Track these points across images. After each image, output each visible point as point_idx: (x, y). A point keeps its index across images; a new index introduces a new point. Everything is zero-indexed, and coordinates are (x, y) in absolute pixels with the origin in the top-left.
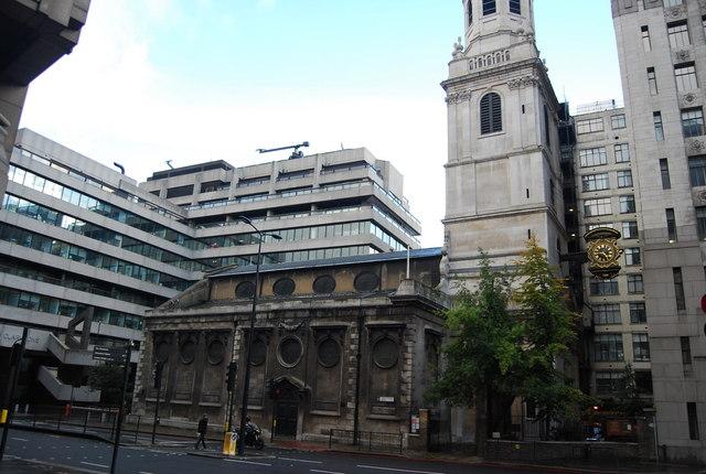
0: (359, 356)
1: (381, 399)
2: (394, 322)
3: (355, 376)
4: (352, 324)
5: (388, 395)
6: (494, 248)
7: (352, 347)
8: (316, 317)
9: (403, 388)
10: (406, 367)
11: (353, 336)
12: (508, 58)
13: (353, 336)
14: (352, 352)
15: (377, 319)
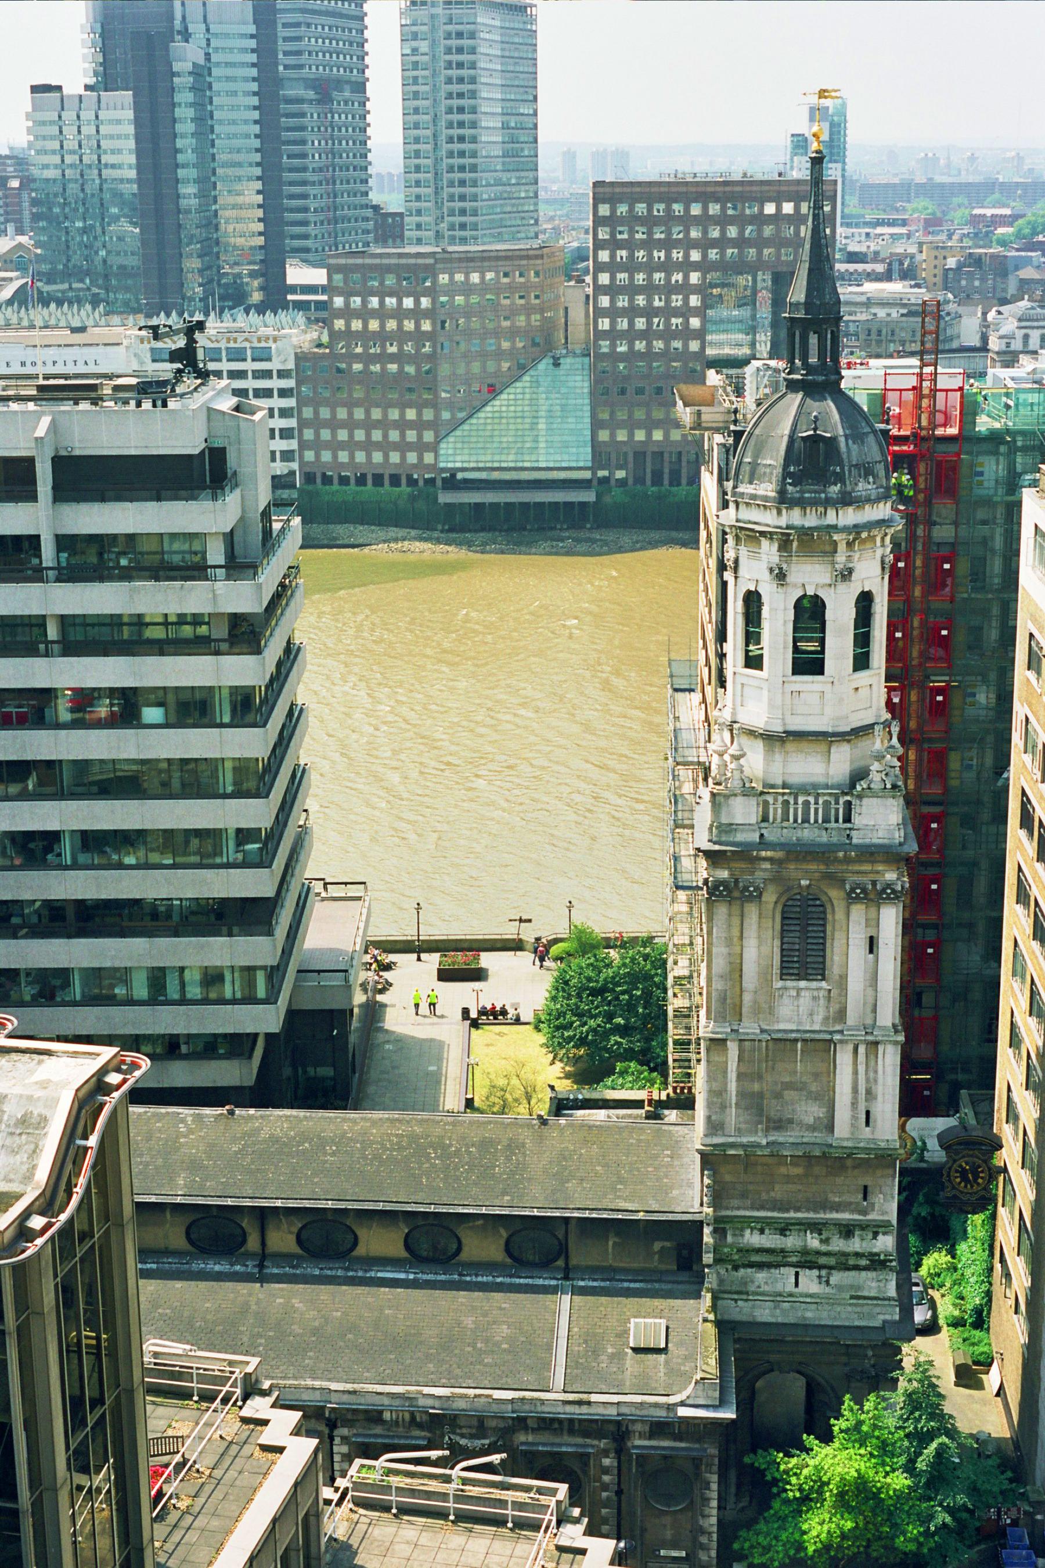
0: (619, 1493)
1: (663, 1553)
2: (683, 1445)
3: (613, 1521)
4: (603, 1444)
5: (675, 1546)
6: (797, 1209)
7: (606, 1478)
8: (526, 1428)
9: (704, 1540)
10: (707, 1511)
11: (606, 1462)
12: (848, 819)
13: (606, 1462)
14: (605, 1487)
15: (650, 1439)
